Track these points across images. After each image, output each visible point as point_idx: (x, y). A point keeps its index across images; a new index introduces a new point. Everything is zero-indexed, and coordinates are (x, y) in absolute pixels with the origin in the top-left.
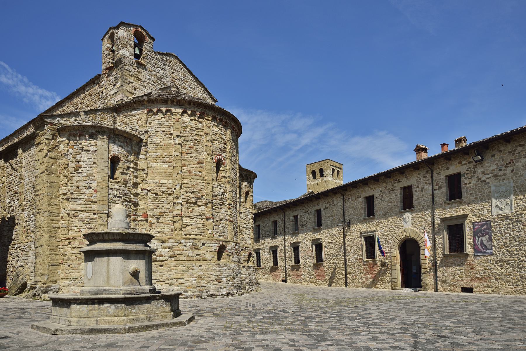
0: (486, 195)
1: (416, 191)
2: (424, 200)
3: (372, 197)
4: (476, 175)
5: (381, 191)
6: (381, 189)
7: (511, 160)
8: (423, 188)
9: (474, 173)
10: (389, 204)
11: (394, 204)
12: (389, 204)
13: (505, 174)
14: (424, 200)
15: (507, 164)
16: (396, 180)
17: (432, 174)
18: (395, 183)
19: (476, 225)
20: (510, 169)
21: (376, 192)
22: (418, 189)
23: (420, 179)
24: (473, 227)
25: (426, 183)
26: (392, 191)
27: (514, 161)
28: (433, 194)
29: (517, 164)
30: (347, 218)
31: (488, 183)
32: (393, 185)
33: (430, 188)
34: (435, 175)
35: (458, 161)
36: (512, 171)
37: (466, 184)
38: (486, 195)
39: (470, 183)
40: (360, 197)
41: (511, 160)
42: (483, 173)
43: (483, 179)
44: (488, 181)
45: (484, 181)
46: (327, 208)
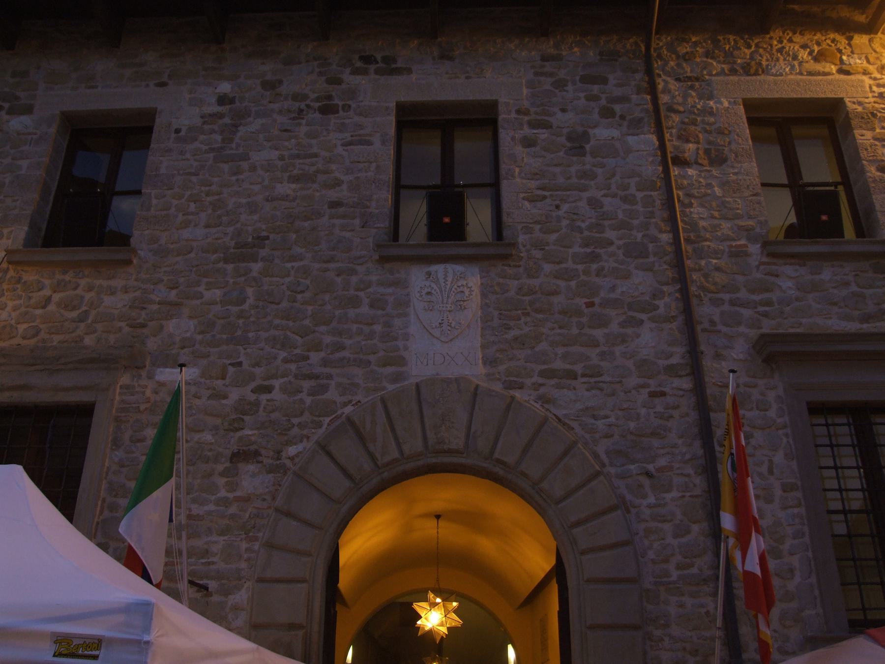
1: (529, 143)
5: (223, 100)
6: (225, 87)
8: (578, 143)
10: (286, 188)
12: (286, 188)
14: (594, 203)
16: (368, 59)
17: (649, 71)
18: (356, 72)
22: (543, 135)
23: (560, 84)
25: (607, 113)
26: (327, 110)
32: (335, 81)
33: (645, 141)
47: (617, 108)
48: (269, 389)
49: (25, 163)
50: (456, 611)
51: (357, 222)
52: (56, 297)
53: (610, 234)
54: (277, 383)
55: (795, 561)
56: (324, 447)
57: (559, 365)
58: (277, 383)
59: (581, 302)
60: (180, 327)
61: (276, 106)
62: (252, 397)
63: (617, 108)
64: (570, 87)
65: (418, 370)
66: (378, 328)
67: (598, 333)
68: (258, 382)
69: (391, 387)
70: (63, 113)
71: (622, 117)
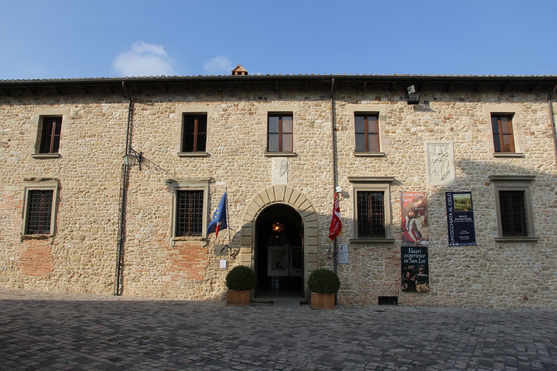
0: (418, 154)
2: (315, 142)
3: (202, 118)
4: (403, 122)
7: (450, 115)
9: (401, 119)
11: (253, 138)
13: (442, 132)
14: (315, 142)
15: (445, 118)
19: (405, 197)
20: (448, 126)
21: (214, 110)
24: (401, 198)
25: (320, 115)
27: (454, 117)
28: (334, 137)
29: (457, 122)
30: (135, 147)
31: (421, 139)
34: (337, 106)
35: (375, 95)
36: (452, 129)
37: (387, 132)
38: (418, 154)
39: (395, 132)
40: (174, 112)
41: (450, 115)
42: (413, 122)
43: (413, 130)
44: (419, 134)
45: (414, 134)
46: (81, 117)
47: (323, 114)
48: (241, 187)
49: (176, 128)
50: (283, 226)
51: (259, 146)
52: (190, 164)
53: (318, 150)
54: (243, 186)
55: (350, 224)
56: (254, 201)
57: (304, 182)
58: (243, 186)
59: (310, 167)
60: (220, 172)
61: (238, 112)
62: (238, 189)
63: (323, 114)
64: (311, 108)
65: (273, 183)
66: (265, 173)
67: (314, 175)
68: (239, 185)
69: (268, 187)
70: (183, 113)
71: (324, 117)
